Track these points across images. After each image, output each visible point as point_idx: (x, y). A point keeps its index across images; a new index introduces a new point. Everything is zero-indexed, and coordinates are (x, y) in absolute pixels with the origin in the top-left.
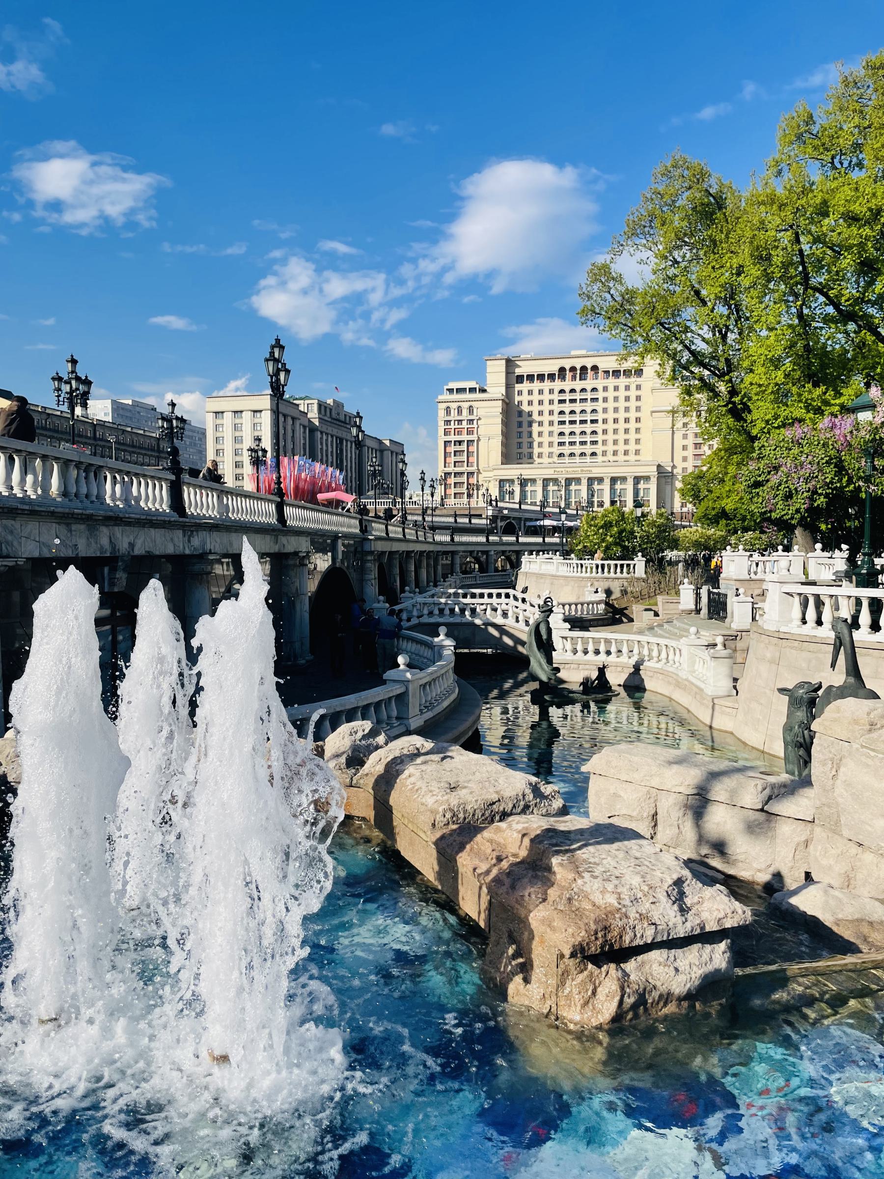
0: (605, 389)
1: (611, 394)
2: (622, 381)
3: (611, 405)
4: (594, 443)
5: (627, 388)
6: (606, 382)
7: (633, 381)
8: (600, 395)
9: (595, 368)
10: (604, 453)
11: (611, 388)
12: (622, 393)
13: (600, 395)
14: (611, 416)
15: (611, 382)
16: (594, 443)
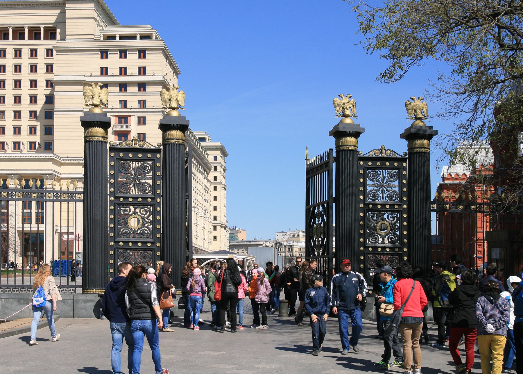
2: (26, 45)
5: (34, 53)
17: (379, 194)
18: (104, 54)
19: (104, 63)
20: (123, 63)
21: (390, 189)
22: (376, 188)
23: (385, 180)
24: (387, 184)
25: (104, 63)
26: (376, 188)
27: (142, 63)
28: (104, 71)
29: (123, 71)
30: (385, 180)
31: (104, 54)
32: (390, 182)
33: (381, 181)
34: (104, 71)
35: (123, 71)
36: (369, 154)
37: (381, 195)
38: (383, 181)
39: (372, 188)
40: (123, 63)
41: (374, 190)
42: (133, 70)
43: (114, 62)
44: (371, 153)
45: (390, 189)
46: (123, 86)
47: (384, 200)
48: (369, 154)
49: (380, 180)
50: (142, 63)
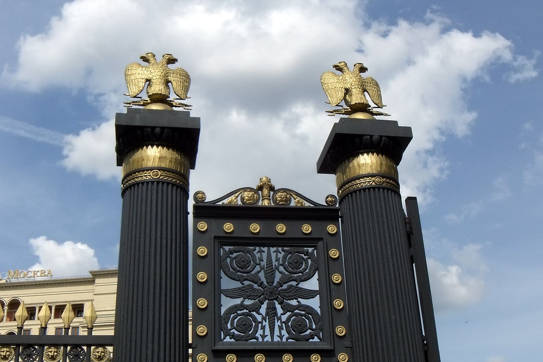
17: (259, 318)
21: (294, 302)
22: (248, 302)
23: (278, 277)
24: (285, 286)
26: (248, 302)
30: (278, 277)
32: (294, 283)
33: (263, 279)
36: (226, 201)
37: (266, 324)
38: (271, 281)
39: (238, 301)
41: (242, 306)
44: (233, 197)
45: (294, 302)
47: (276, 339)
48: (226, 201)
49: (262, 275)
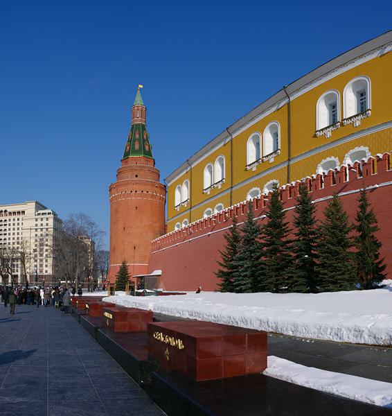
0: (10, 220)
1: (12, 222)
2: (16, 217)
3: (12, 227)
4: (5, 234)
6: (10, 217)
7: (20, 217)
8: (8, 223)
9: (6, 211)
10: (9, 244)
11: (12, 220)
12: (16, 222)
13: (8, 223)
14: (12, 232)
15: (12, 217)
16: (5, 234)
18: (37, 220)
19: (37, 223)
20: (42, 222)
25: (37, 223)
27: (47, 222)
28: (36, 225)
29: (42, 225)
31: (37, 220)
34: (36, 225)
35: (42, 225)
40: (42, 222)
42: (44, 224)
43: (39, 222)
46: (42, 229)
50: (47, 222)
